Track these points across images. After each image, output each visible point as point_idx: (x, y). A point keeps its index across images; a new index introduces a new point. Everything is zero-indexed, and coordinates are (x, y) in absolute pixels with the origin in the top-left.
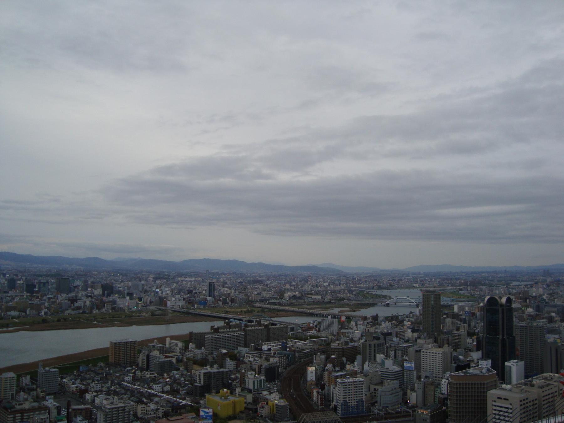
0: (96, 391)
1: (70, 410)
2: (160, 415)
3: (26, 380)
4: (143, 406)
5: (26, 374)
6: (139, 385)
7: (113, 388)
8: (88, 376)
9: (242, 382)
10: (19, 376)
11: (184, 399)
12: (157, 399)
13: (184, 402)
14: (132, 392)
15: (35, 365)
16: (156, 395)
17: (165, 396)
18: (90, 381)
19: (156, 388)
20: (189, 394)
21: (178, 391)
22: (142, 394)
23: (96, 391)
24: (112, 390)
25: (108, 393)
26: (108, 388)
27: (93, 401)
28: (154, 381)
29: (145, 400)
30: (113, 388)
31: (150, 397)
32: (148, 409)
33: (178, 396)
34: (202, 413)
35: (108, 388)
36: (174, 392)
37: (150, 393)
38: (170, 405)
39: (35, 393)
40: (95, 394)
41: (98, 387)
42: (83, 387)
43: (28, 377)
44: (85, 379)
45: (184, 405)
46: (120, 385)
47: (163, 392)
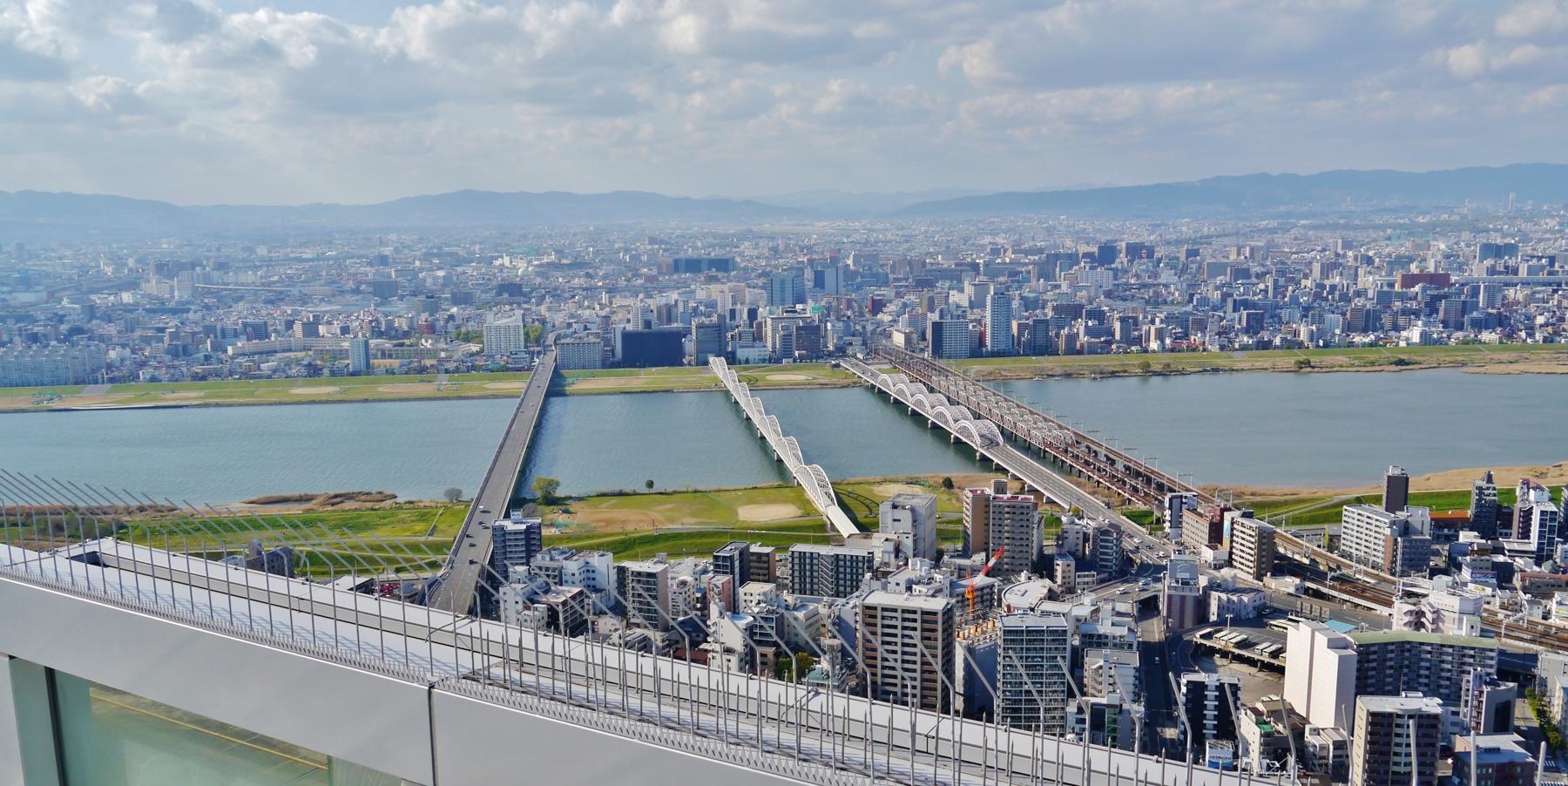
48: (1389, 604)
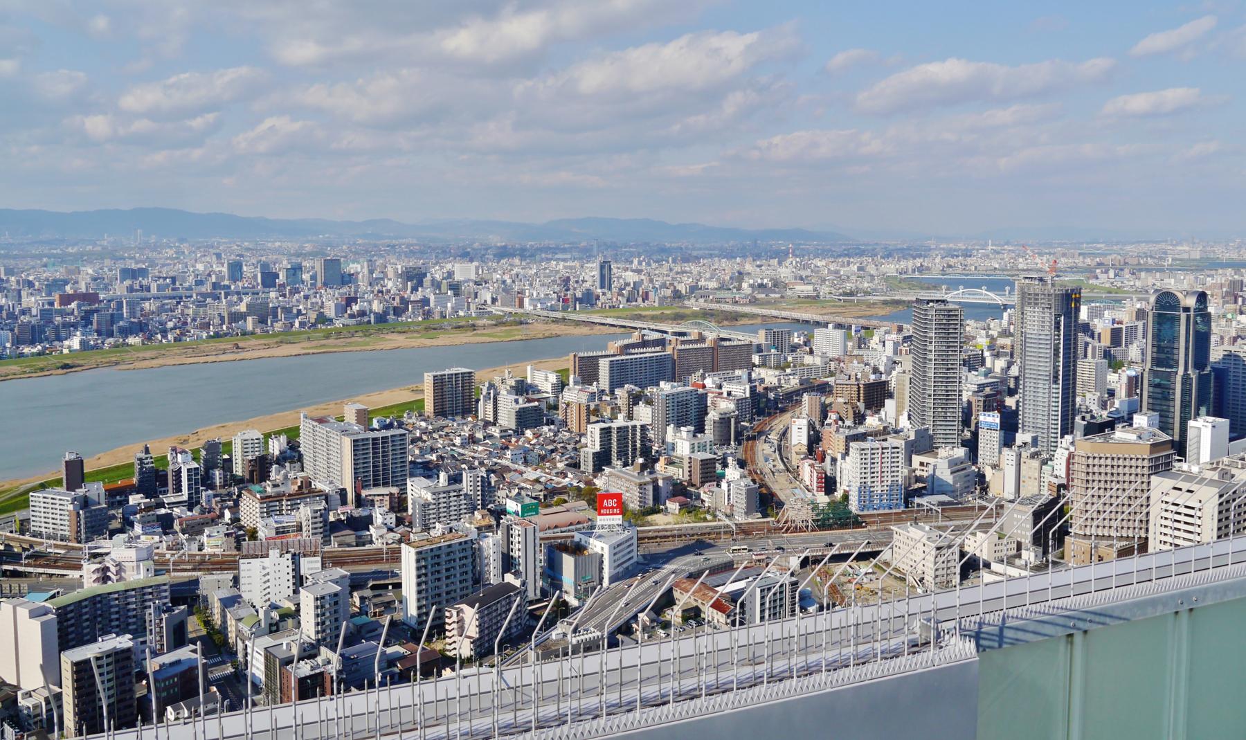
13: (566, 481)
48: (79, 567)
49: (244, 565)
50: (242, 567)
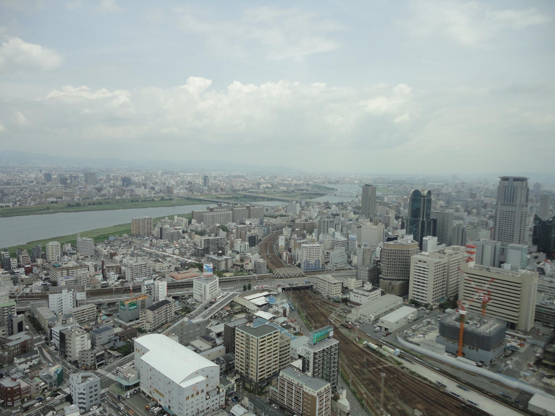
0: (123, 254)
1: (104, 267)
2: (173, 269)
3: (68, 247)
4: (160, 263)
5: (68, 242)
6: (155, 249)
7: (136, 252)
8: (115, 244)
9: (232, 246)
10: (62, 244)
11: (190, 259)
12: (169, 259)
13: (190, 261)
14: (151, 254)
15: (75, 235)
16: (169, 256)
17: (175, 257)
18: (117, 247)
19: (169, 251)
20: (193, 255)
21: (185, 254)
22: (158, 255)
23: (123, 254)
24: (135, 253)
25: (132, 255)
26: (132, 252)
27: (121, 261)
28: (167, 246)
29: (161, 260)
30: (136, 252)
31: (164, 257)
32: (164, 266)
33: (185, 256)
34: (205, 267)
35: (132, 252)
36: (182, 254)
37: (164, 255)
38: (179, 263)
39: (76, 256)
40: (122, 256)
41: (124, 251)
42: (112, 251)
43: (70, 245)
44: (114, 246)
45: (190, 263)
46: (141, 249)
47: (174, 254)
49: (51, 297)
50: (50, 297)
